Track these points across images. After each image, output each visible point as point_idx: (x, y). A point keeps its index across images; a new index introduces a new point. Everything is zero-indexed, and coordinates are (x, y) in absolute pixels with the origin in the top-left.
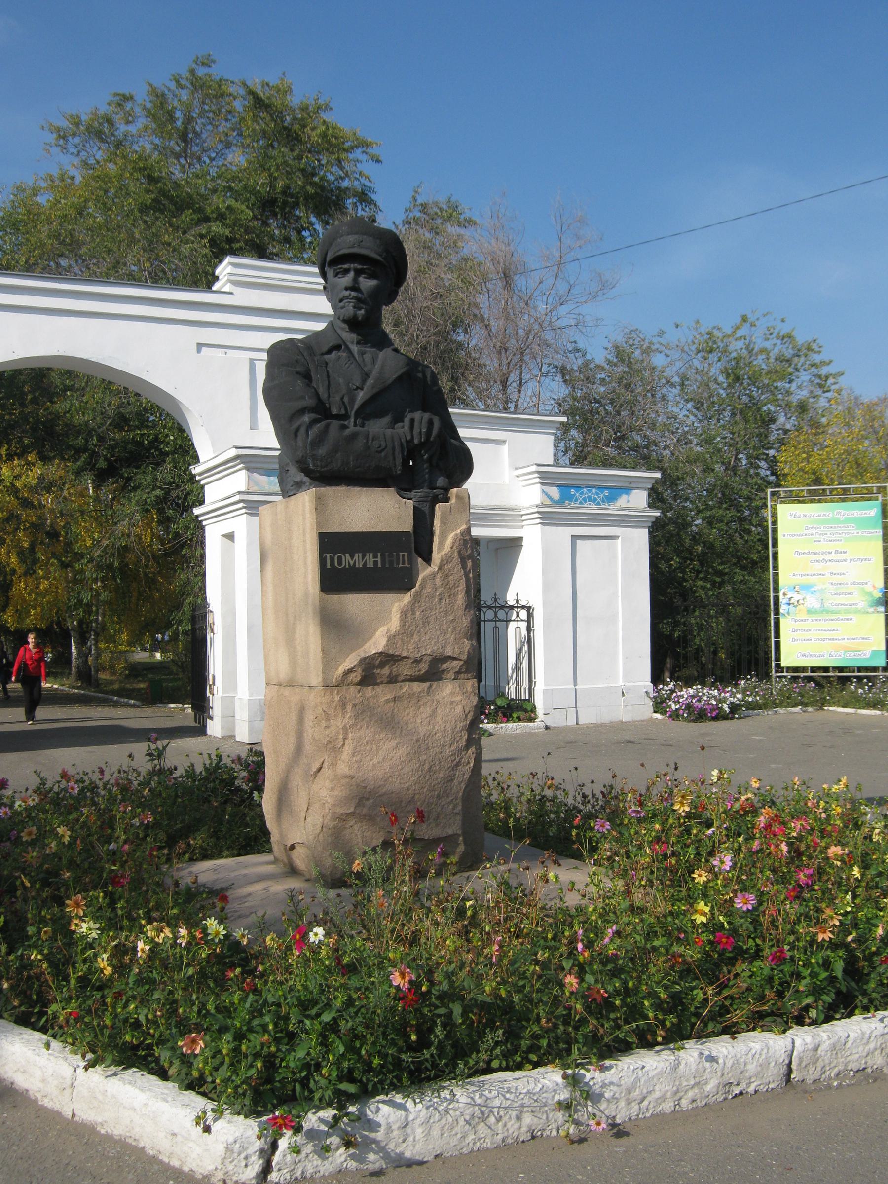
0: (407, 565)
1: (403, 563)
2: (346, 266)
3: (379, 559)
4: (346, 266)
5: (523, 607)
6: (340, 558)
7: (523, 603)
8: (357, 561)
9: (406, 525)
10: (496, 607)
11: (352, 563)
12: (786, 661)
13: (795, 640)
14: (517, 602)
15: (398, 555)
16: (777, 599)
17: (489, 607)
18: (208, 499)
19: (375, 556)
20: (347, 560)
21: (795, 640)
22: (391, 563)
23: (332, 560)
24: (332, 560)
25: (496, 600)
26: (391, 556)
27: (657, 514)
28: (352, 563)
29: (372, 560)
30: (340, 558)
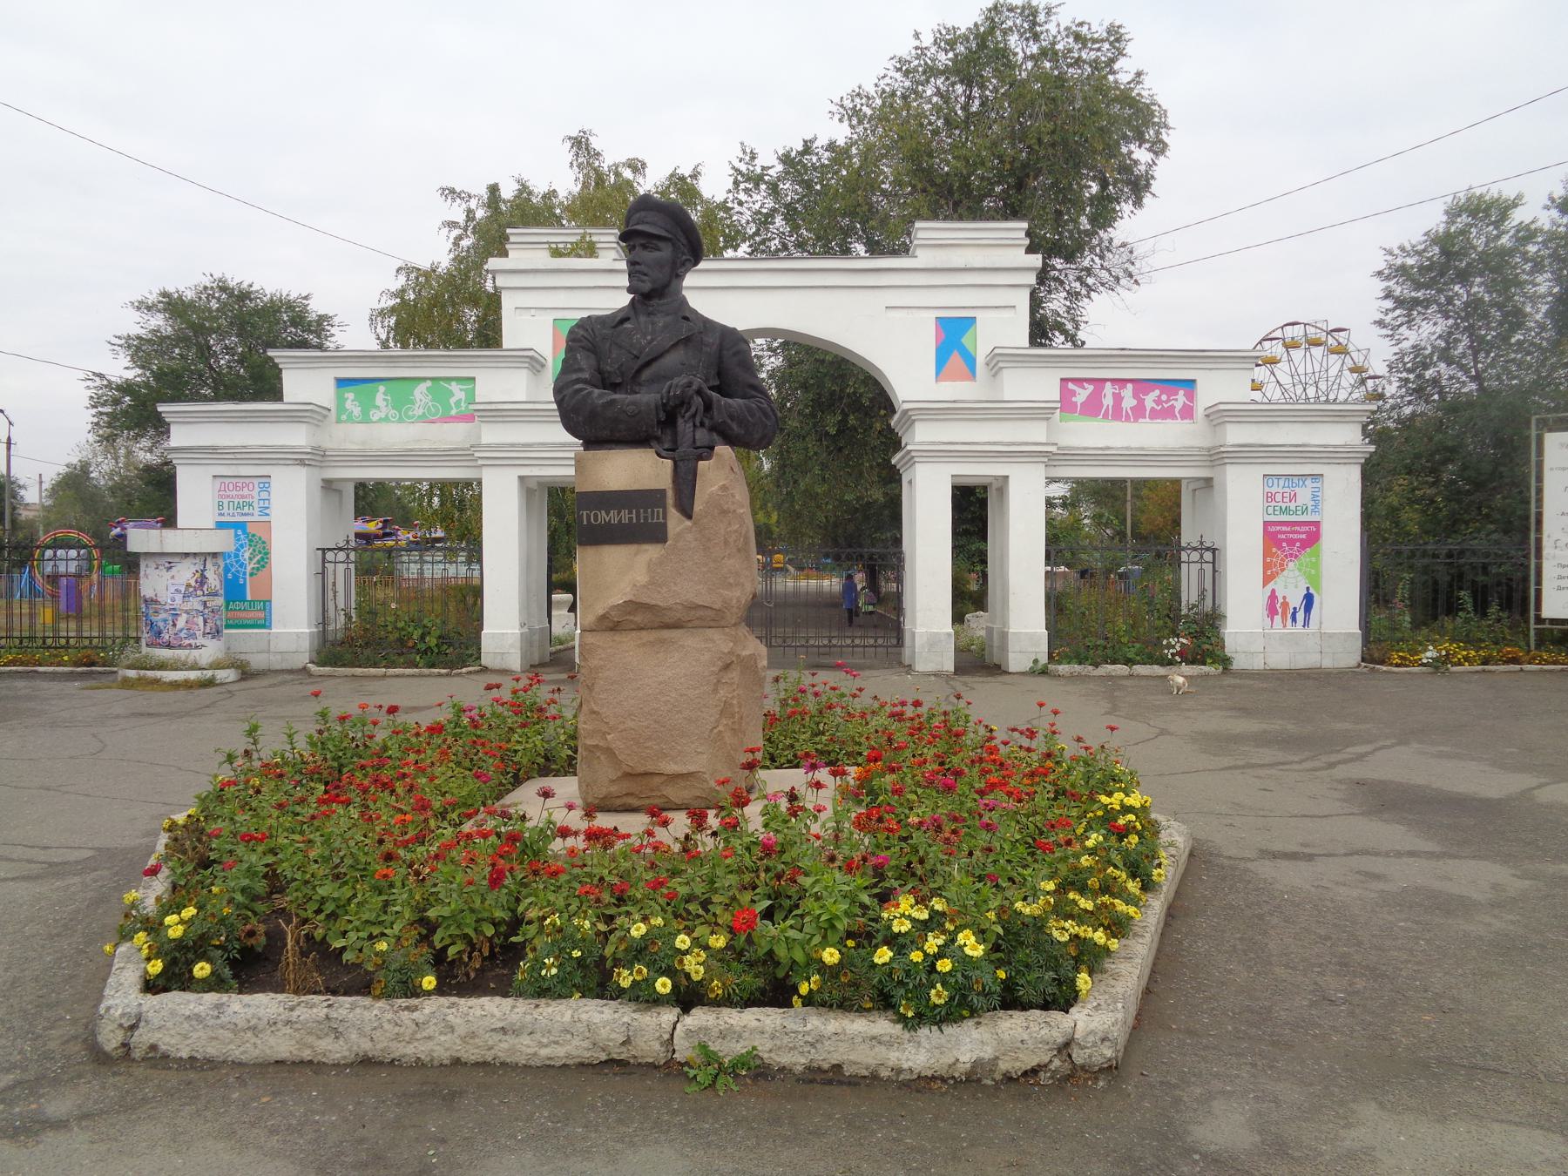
5: (1208, 549)
8: (613, 517)
12: (1548, 612)
13: (1559, 588)
16: (1539, 541)
20: (603, 517)
21: (1559, 588)
22: (646, 518)
23: (588, 517)
24: (588, 517)
27: (1372, 448)
30: (596, 516)
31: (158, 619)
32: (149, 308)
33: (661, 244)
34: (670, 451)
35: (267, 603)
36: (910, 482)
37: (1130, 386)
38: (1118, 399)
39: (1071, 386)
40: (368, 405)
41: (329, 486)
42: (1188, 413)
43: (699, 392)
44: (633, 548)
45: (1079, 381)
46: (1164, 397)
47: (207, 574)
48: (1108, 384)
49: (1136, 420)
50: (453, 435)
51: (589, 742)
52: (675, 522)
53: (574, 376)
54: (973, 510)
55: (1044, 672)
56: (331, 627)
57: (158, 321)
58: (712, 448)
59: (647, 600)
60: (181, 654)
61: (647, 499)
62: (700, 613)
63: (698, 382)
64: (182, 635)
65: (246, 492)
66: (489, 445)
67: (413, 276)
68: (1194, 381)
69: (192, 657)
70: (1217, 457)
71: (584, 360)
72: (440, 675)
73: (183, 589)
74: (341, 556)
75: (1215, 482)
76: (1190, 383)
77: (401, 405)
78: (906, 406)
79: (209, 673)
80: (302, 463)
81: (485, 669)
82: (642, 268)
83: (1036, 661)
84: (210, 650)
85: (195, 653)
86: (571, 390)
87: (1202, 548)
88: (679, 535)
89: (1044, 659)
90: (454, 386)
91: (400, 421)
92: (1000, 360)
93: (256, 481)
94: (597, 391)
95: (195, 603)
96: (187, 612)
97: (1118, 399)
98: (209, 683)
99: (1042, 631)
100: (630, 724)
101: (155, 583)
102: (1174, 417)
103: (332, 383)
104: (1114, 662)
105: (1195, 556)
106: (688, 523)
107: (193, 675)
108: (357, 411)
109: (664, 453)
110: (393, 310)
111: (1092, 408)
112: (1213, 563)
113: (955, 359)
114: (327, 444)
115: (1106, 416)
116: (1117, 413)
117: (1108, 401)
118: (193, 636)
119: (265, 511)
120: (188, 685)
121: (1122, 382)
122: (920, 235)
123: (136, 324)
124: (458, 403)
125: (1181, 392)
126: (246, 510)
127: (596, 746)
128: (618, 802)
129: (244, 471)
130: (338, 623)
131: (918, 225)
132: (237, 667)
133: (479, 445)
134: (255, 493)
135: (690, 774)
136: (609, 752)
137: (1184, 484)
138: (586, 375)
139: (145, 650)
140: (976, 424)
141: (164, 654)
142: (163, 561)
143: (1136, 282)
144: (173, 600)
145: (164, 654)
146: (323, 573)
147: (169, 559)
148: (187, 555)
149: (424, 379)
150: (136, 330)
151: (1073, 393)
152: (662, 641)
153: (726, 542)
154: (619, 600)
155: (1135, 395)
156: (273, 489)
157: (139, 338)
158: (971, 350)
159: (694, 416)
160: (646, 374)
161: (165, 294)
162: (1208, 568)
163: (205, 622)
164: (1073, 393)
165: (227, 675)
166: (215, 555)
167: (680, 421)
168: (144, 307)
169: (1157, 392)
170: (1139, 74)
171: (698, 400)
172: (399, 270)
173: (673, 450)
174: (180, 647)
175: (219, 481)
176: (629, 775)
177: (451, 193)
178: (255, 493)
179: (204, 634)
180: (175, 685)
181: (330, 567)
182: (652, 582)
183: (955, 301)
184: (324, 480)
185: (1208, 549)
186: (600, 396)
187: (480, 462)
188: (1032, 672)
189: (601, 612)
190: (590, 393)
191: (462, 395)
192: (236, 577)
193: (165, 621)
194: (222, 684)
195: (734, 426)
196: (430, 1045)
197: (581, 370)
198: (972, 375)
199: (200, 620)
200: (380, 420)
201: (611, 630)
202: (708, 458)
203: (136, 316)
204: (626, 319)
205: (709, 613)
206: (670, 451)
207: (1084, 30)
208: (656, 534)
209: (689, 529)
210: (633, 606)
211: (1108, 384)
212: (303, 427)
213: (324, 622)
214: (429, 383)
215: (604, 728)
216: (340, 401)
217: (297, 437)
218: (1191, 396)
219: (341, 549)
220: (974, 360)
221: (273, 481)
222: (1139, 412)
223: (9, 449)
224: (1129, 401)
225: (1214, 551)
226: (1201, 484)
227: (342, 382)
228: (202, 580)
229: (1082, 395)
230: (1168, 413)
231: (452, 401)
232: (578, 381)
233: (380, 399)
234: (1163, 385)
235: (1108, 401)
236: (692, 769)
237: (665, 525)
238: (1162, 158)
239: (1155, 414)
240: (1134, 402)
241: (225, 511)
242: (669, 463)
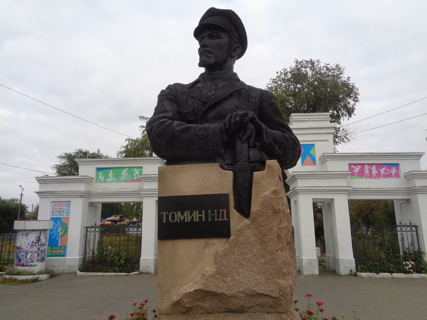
0: (225, 219)
1: (223, 217)
2: (202, 36)
3: (203, 215)
4: (202, 36)
5: (413, 226)
6: (173, 215)
7: (413, 224)
8: (187, 217)
10: (401, 226)
11: (182, 219)
14: (411, 224)
15: (218, 212)
18: (291, 189)
19: (200, 213)
22: (213, 217)
23: (167, 216)
24: (167, 216)
25: (401, 223)
26: (213, 212)
28: (182, 219)
29: (198, 216)
30: (173, 215)
31: (20, 255)
32: (62, 158)
33: (222, 34)
35: (65, 247)
36: (295, 202)
37: (374, 166)
38: (370, 171)
39: (352, 166)
40: (106, 177)
41: (91, 205)
42: (397, 175)
43: (253, 121)
44: (201, 242)
45: (355, 165)
46: (388, 170)
47: (41, 237)
48: (366, 166)
49: (378, 178)
50: (133, 186)
53: (161, 115)
54: (319, 212)
55: (355, 275)
56: (88, 256)
57: (64, 161)
58: (264, 163)
59: (213, 289)
60: (27, 268)
61: (216, 202)
62: (260, 300)
63: (251, 114)
64: (29, 261)
65: (62, 207)
66: (146, 190)
67: (130, 142)
68: (398, 164)
69: (31, 270)
70: (412, 191)
71: (168, 106)
72: (124, 275)
73: (31, 243)
74: (93, 230)
75: (412, 200)
77: (117, 177)
79: (36, 276)
80: (82, 197)
81: (141, 273)
82: (209, 49)
83: (351, 271)
84: (39, 267)
85: (33, 268)
86: (157, 123)
87: (411, 226)
88: (240, 232)
89: (354, 270)
90: (136, 170)
91: (117, 182)
92: (325, 158)
93: (66, 203)
94: (176, 122)
95: (35, 249)
96: (31, 252)
97: (370, 171)
98: (36, 280)
99: (353, 259)
101: (22, 242)
102: (392, 177)
103: (95, 170)
104: (384, 272)
105: (409, 229)
106: (247, 221)
107: (30, 277)
108: (103, 179)
109: (226, 167)
110: (124, 152)
111: (361, 174)
112: (417, 231)
114: (92, 190)
115: (366, 177)
116: (371, 176)
117: (367, 171)
118: (33, 261)
119: (68, 214)
120: (27, 282)
121: (371, 165)
122: (293, 118)
123: (59, 162)
124: (136, 175)
125: (394, 168)
126: (61, 213)
129: (62, 200)
130: (89, 255)
131: (292, 114)
132: (48, 273)
133: (142, 190)
134: (65, 207)
137: (395, 202)
138: (170, 114)
139: (15, 267)
141: (21, 268)
142: (25, 233)
143: (349, 140)
144: (27, 247)
145: (21, 268)
146: (86, 236)
147: (27, 232)
148: (34, 230)
149: (126, 168)
150: (59, 163)
151: (354, 169)
153: (279, 237)
154: (189, 287)
155: (377, 169)
156: (71, 206)
157: (60, 166)
158: (314, 156)
159: (248, 139)
160: (211, 115)
161: (66, 154)
162: (414, 233)
163: (38, 255)
164: (354, 169)
165: (42, 277)
166: (45, 230)
167: (238, 142)
168: (61, 157)
169: (385, 168)
170: (349, 78)
171: (251, 126)
172: (126, 140)
173: (233, 165)
174: (27, 266)
175: (53, 203)
177: (142, 118)
178: (65, 207)
179: (37, 261)
180: (22, 282)
181: (89, 233)
182: (219, 273)
184: (89, 203)
185: (413, 226)
186: (178, 125)
187: (143, 195)
188: (350, 275)
189: (175, 298)
190: (171, 124)
191: (138, 173)
192: (55, 238)
193: (23, 255)
194: (41, 280)
195: (277, 148)
198: (314, 163)
199: (36, 255)
200: (110, 182)
201: (184, 313)
203: (59, 160)
205: (267, 300)
206: (231, 165)
207: (329, 66)
209: (248, 227)
210: (202, 294)
211: (366, 166)
212: (84, 184)
213: (85, 254)
214: (127, 169)
216: (97, 175)
217: (81, 188)
218: (398, 169)
219: (93, 227)
220: (315, 159)
221: (71, 203)
222: (379, 175)
223: (21, 197)
224: (375, 172)
225: (416, 227)
226: (404, 201)
227: (98, 169)
228: (39, 240)
229: (357, 169)
230: (390, 176)
231: (135, 175)
233: (110, 175)
234: (386, 164)
235: (367, 171)
237: (228, 223)
238: (357, 103)
239: (385, 176)
240: (377, 172)
241: (54, 214)
242: (230, 174)
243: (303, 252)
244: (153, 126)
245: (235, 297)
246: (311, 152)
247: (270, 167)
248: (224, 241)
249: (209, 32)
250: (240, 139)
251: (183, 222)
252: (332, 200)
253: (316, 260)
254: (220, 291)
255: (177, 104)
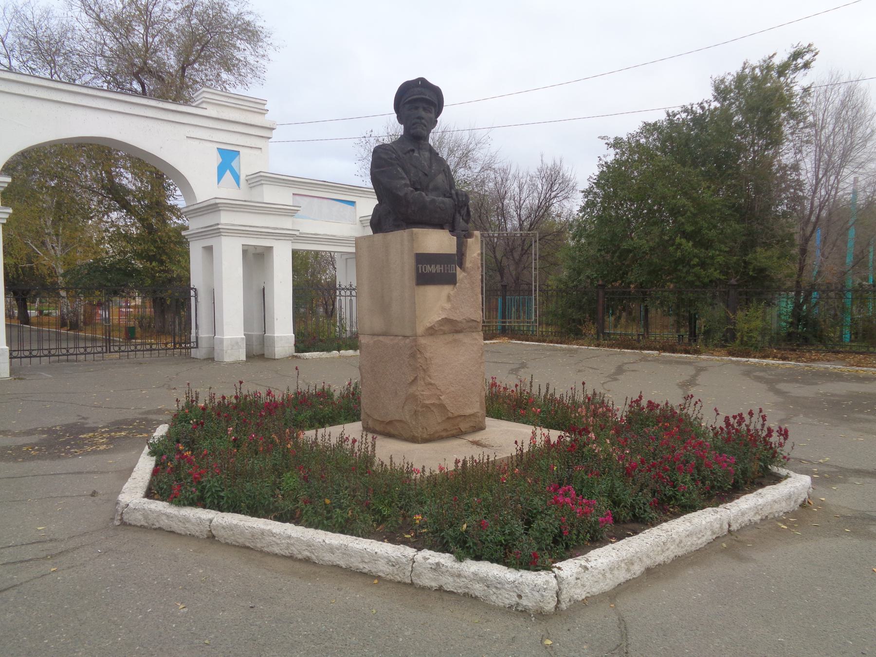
9: (453, 250)
17: (348, 289)
34: (452, 231)
36: (209, 249)
51: (427, 402)
52: (460, 275)
53: (403, 182)
59: (452, 317)
76: (352, 203)
78: (218, 201)
99: (291, 335)
100: (453, 389)
113: (228, 175)
127: (433, 404)
128: (437, 435)
135: (473, 415)
136: (442, 407)
140: (241, 214)
152: (455, 341)
167: (458, 215)
176: (449, 418)
183: (231, 140)
189: (429, 325)
196: (667, 554)
197: (403, 178)
201: (432, 335)
202: (470, 236)
204: (413, 151)
205: (475, 324)
208: (451, 280)
210: (446, 321)
215: (439, 393)
232: (406, 185)
236: (475, 410)
243: (225, 327)
244: (406, 194)
245: (461, 322)
246: (234, 164)
247: (477, 237)
248: (451, 287)
249: (425, 106)
250: (460, 213)
251: (431, 272)
252: (270, 249)
253: (242, 338)
254: (455, 319)
255: (403, 169)
